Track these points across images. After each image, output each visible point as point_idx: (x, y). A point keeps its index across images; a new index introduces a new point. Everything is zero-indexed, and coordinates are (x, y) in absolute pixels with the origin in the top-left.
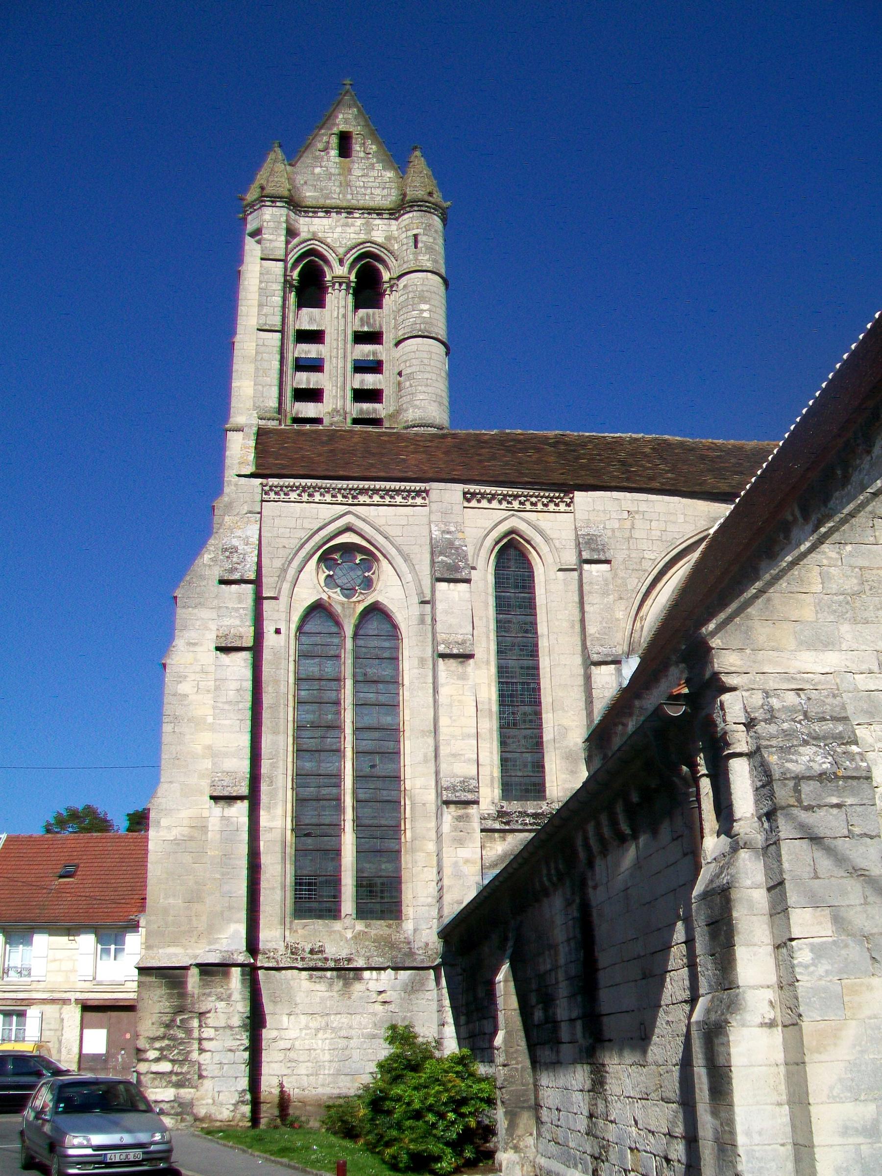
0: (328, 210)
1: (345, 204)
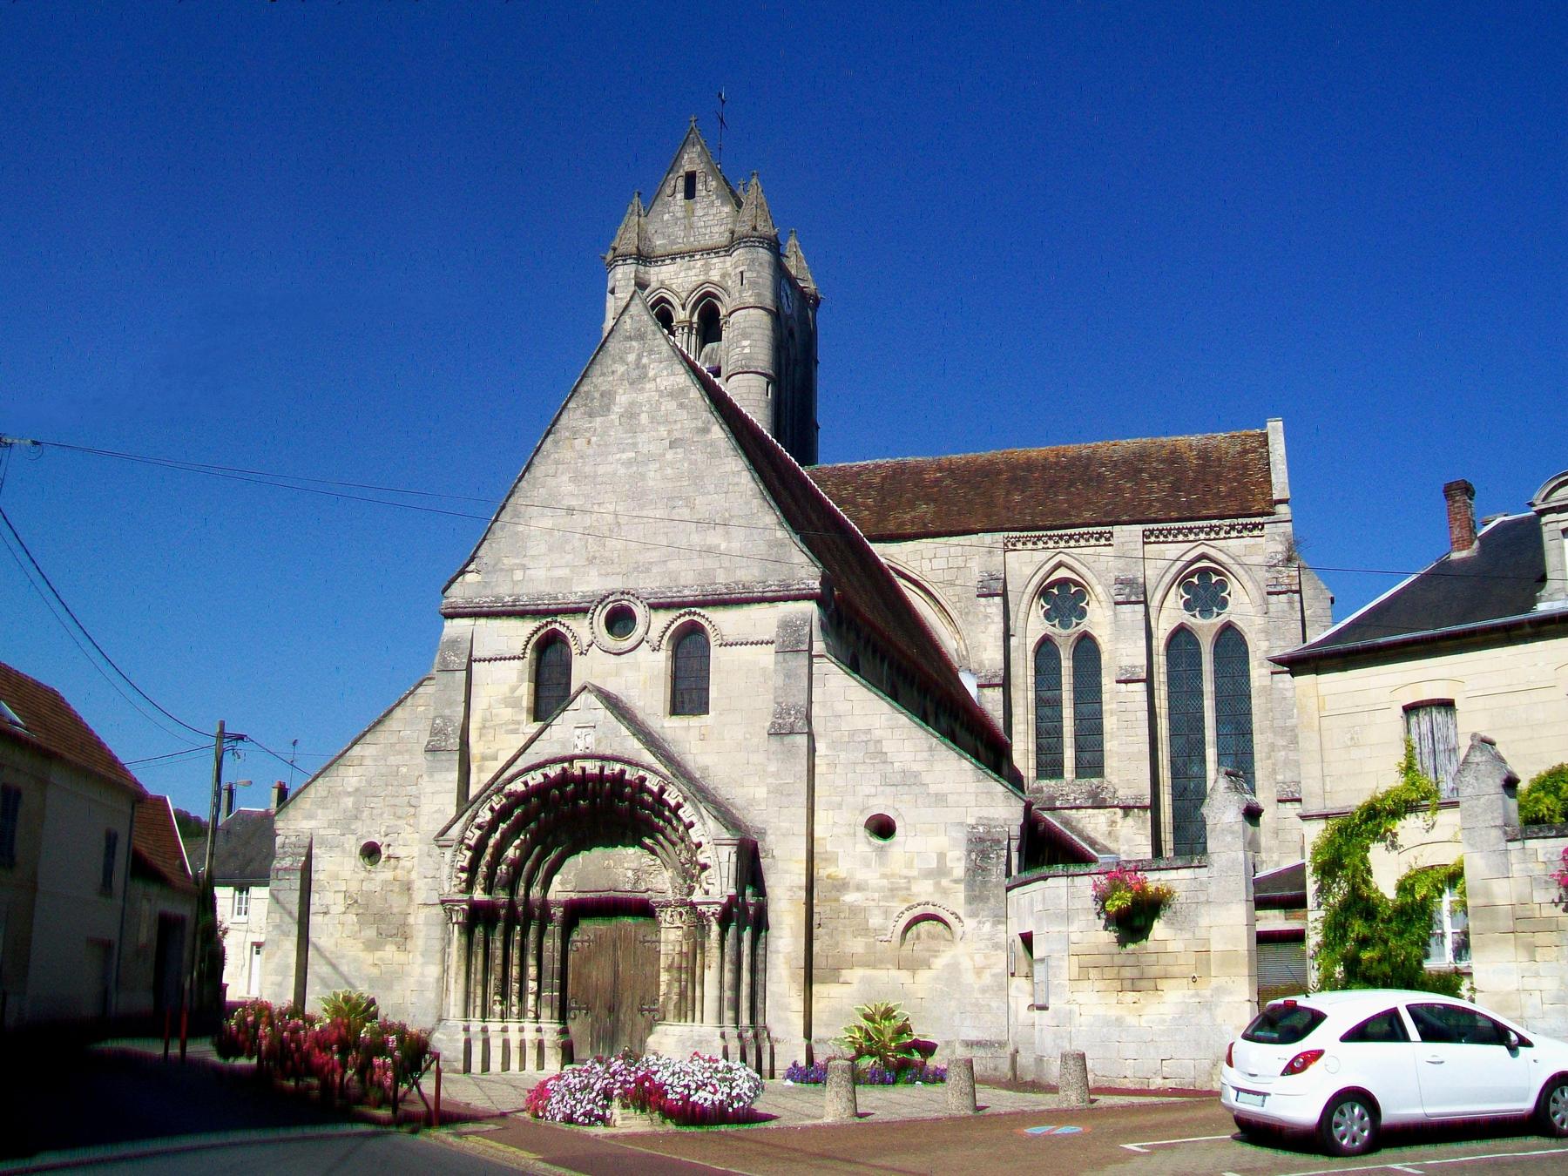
0: (673, 257)
1: (687, 248)
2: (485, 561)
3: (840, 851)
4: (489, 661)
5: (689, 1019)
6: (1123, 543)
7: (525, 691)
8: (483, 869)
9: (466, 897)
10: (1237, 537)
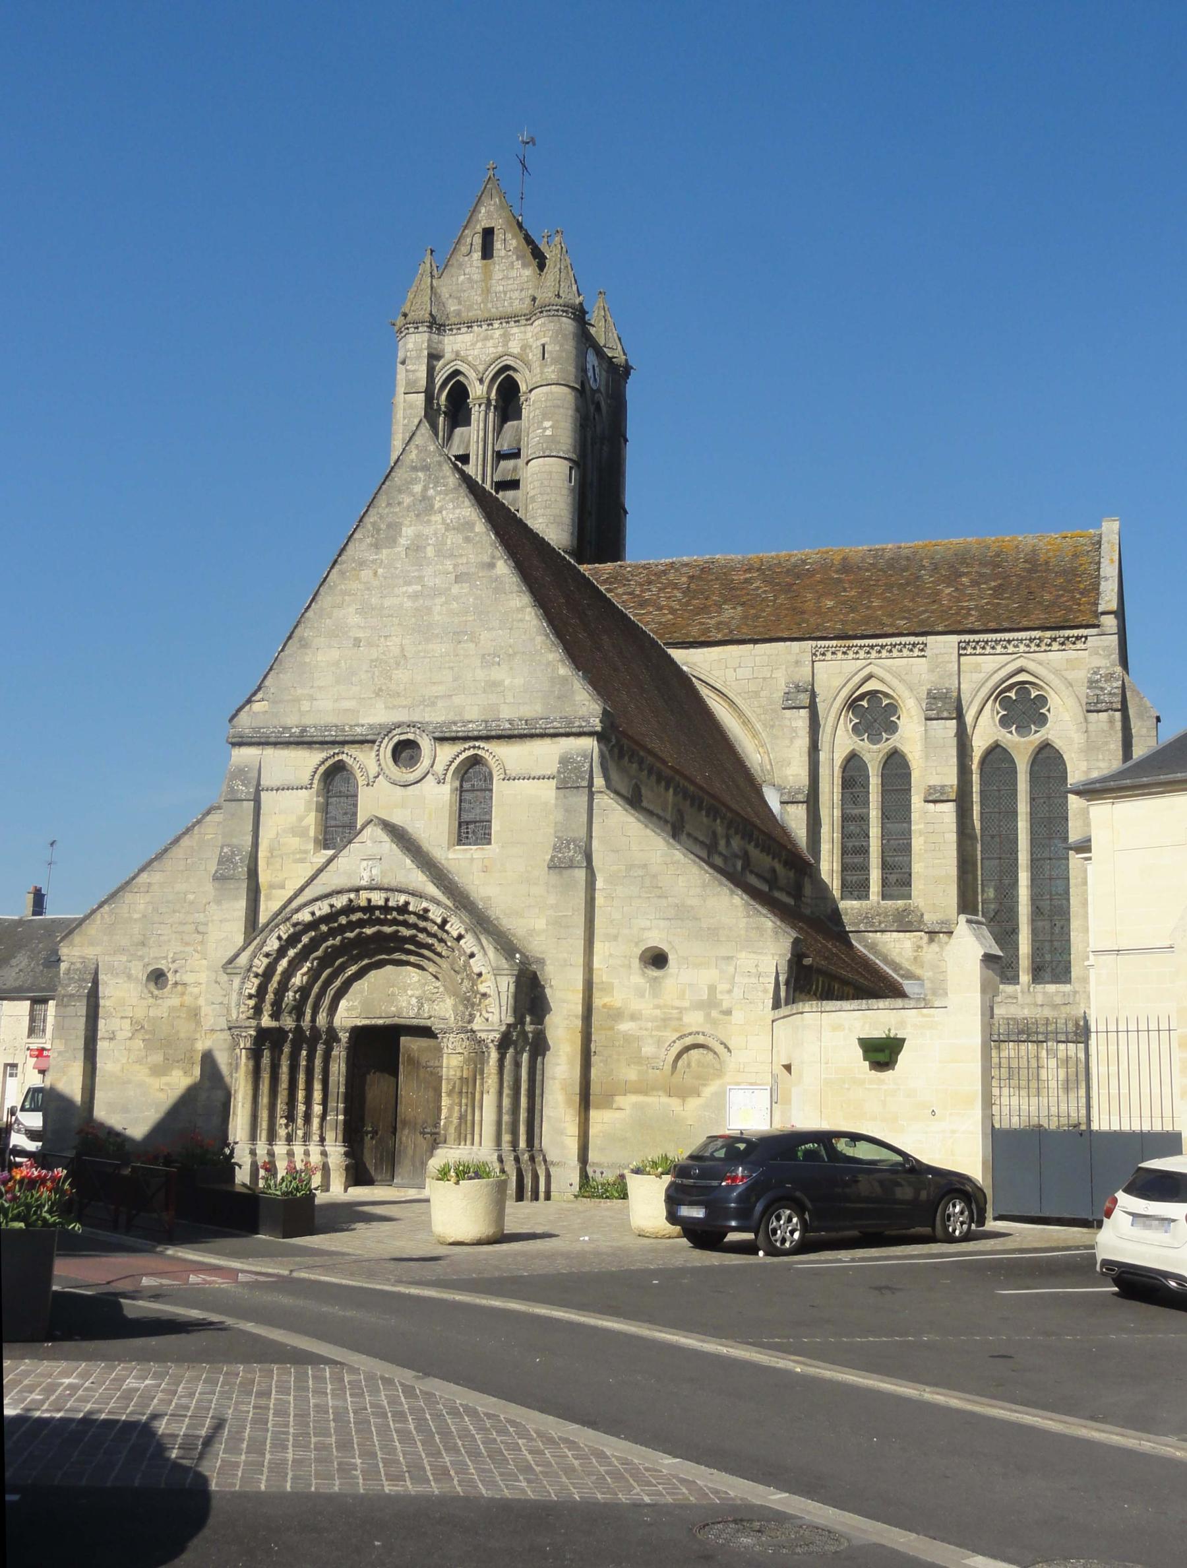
1: (486, 315)
2: (272, 690)
3: (616, 982)
4: (277, 790)
5: (468, 1142)
6: (937, 655)
7: (311, 820)
8: (270, 997)
9: (253, 1023)
10: (1058, 650)
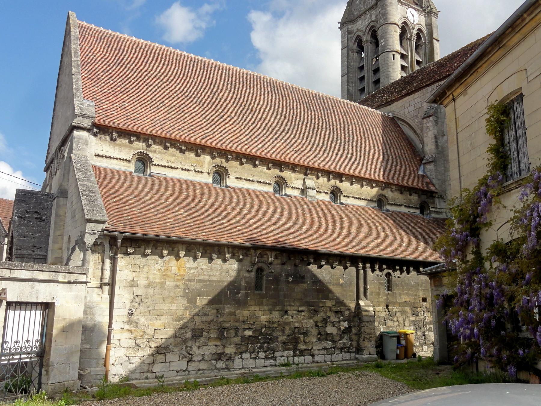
0: (359, 17)
